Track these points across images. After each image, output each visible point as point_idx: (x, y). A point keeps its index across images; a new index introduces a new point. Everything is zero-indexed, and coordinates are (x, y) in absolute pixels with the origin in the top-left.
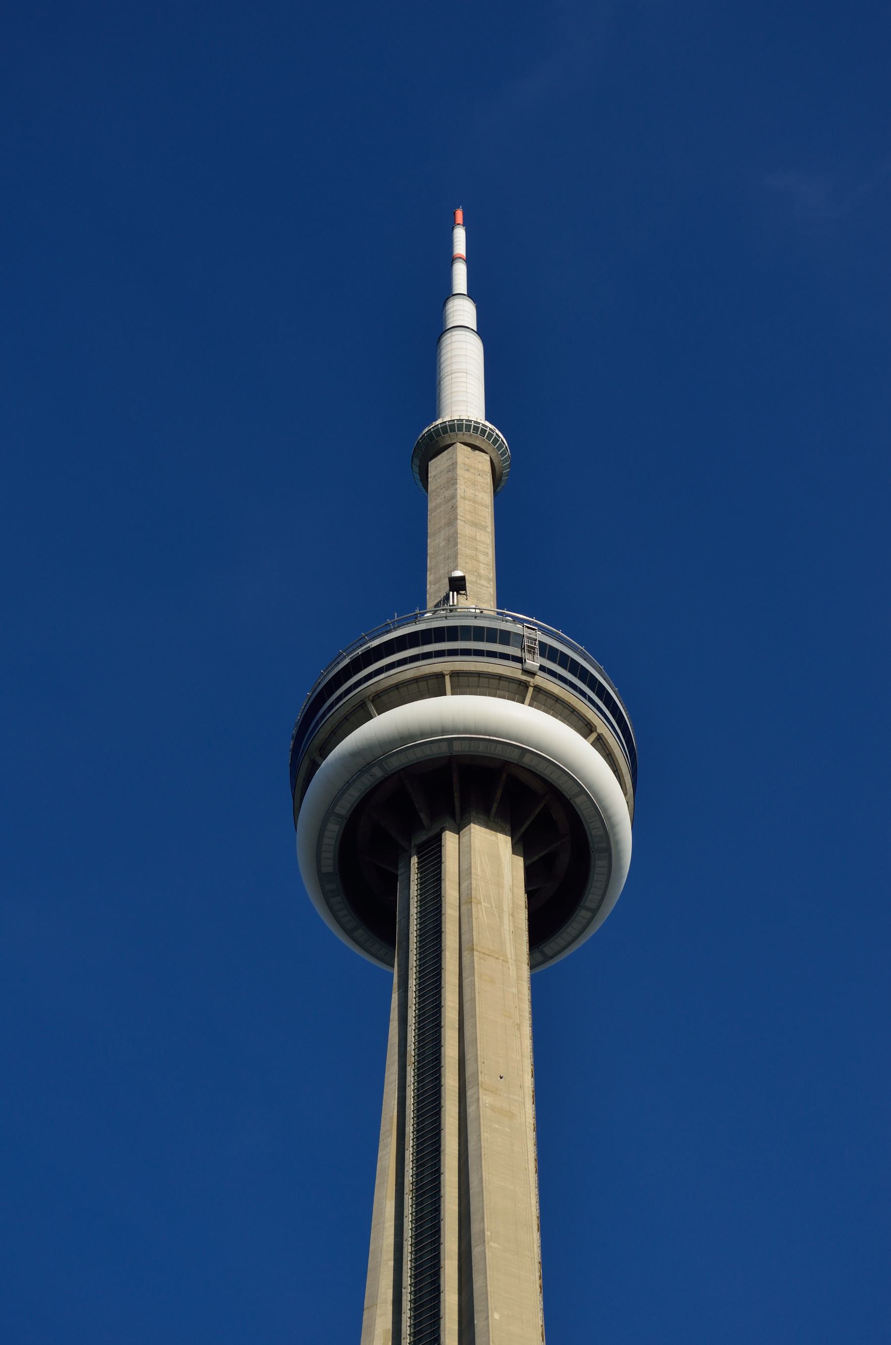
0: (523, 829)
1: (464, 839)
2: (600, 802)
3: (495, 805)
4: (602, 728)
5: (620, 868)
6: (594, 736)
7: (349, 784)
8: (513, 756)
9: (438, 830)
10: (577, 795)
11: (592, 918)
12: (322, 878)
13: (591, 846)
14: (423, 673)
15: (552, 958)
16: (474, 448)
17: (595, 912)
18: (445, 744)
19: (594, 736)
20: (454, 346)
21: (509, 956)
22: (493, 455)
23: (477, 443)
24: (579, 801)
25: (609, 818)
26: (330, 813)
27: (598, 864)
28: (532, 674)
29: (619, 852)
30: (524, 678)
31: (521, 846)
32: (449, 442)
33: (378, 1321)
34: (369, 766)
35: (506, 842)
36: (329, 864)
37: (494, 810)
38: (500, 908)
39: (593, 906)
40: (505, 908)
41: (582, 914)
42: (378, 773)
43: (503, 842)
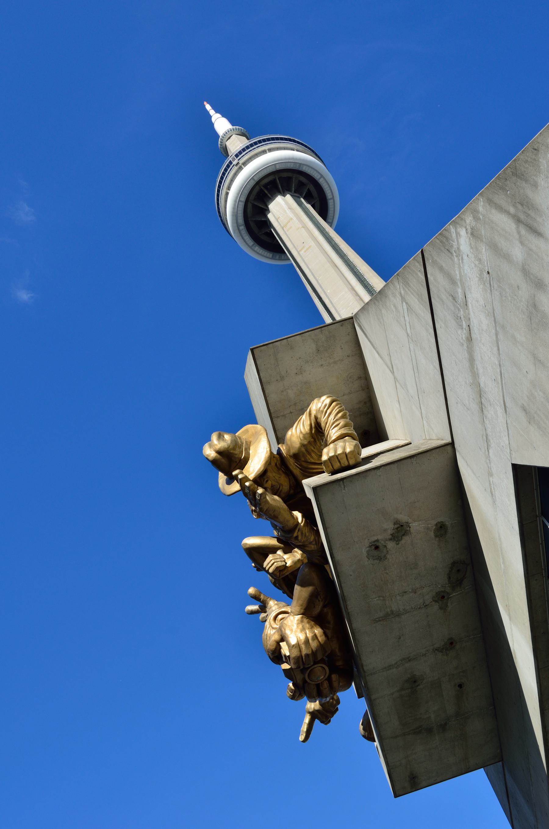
0: (281, 189)
2: (282, 160)
3: (269, 195)
5: (310, 162)
6: (267, 151)
7: (243, 238)
8: (253, 183)
10: (275, 167)
11: (324, 178)
12: (273, 258)
16: (229, 138)
17: (322, 176)
18: (240, 203)
19: (267, 151)
24: (278, 167)
25: (289, 159)
26: (251, 247)
27: (305, 169)
28: (238, 163)
29: (304, 160)
34: (238, 229)
36: (270, 255)
39: (319, 176)
40: (286, 209)
42: (242, 228)
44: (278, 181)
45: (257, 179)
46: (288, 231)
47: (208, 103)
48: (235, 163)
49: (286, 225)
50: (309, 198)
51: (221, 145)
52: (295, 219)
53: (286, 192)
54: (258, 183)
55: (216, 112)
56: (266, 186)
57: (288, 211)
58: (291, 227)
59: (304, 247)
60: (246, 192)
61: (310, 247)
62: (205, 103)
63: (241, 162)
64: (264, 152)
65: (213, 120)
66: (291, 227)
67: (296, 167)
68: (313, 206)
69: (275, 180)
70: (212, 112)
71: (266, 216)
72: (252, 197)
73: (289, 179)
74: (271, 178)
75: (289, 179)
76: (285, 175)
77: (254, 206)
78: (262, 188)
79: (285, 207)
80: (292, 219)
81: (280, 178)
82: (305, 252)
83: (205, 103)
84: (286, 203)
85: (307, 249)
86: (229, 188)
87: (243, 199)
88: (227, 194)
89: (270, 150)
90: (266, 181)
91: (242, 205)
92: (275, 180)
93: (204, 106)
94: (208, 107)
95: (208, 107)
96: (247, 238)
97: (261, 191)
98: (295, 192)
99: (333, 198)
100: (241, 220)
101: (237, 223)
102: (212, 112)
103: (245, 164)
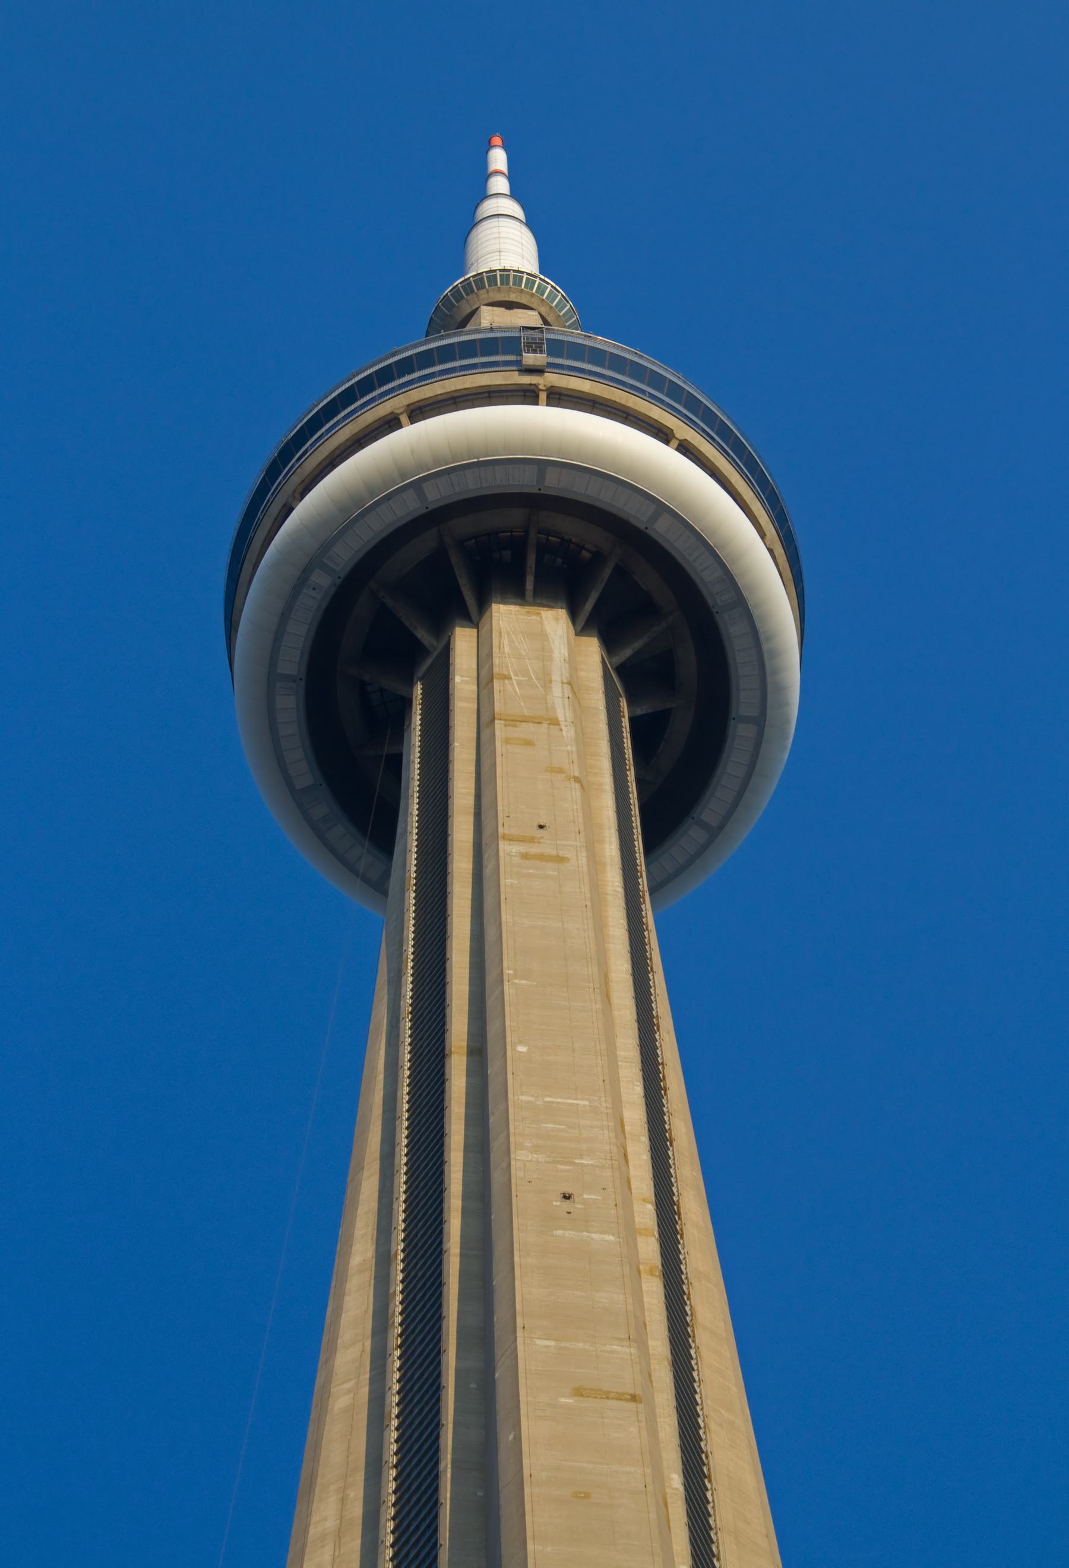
0: (589, 606)
1: (484, 631)
4: (683, 431)
7: (284, 617)
8: (524, 482)
9: (446, 639)
10: (655, 517)
13: (710, 602)
14: (364, 425)
15: (721, 827)
20: (480, 236)
21: (561, 718)
22: (544, 310)
23: (513, 297)
24: (661, 530)
26: (272, 678)
27: (733, 631)
28: (538, 371)
30: (527, 380)
31: (586, 623)
32: (468, 310)
33: (363, 1185)
34: (306, 573)
35: (557, 620)
37: (529, 585)
38: (547, 681)
40: (556, 677)
42: (323, 582)
43: (555, 622)
44: (607, 572)
45: (554, 484)
46: (507, 741)
47: (505, 147)
48: (530, 359)
49: (513, 721)
51: (456, 292)
52: (568, 732)
54: (536, 502)
57: (558, 692)
58: (529, 743)
59: (532, 840)
60: (471, 486)
61: (560, 859)
62: (497, 140)
63: (552, 379)
64: (663, 434)
66: (529, 743)
67: (717, 598)
68: (638, 781)
69: (598, 557)
70: (500, 184)
72: (464, 526)
73: (645, 609)
74: (593, 537)
75: (645, 609)
76: (649, 580)
78: (533, 536)
79: (559, 672)
80: (554, 722)
81: (620, 571)
82: (525, 856)
83: (497, 140)
84: (572, 662)
85: (541, 857)
86: (419, 412)
87: (436, 496)
88: (391, 424)
89: (685, 449)
90: (569, 527)
91: (410, 508)
93: (490, 146)
94: (498, 158)
95: (498, 158)
96: (300, 633)
98: (620, 670)
100: (346, 555)
101: (326, 547)
102: (500, 184)
103: (559, 398)
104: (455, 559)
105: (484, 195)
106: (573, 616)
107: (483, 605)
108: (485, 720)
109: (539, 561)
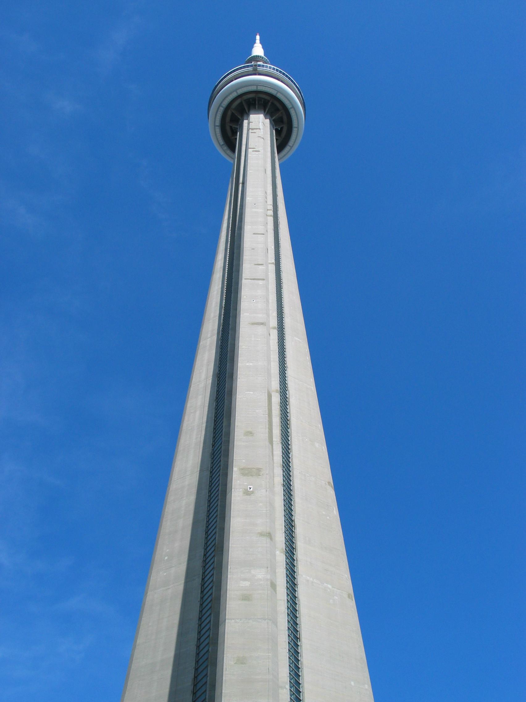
17: (298, 128)
41: (295, 131)
50: (278, 133)
53: (268, 116)
55: (261, 43)
56: (260, 99)
65: (255, 45)
69: (269, 101)
71: (242, 116)
72: (245, 97)
73: (278, 110)
75: (278, 110)
77: (241, 103)
81: (272, 103)
92: (269, 101)
94: (258, 37)
95: (258, 37)
97: (254, 99)
98: (274, 120)
99: (292, 147)
104: (244, 103)
105: (255, 43)
106: (265, 112)
107: (249, 111)
108: (248, 130)
109: (258, 103)
